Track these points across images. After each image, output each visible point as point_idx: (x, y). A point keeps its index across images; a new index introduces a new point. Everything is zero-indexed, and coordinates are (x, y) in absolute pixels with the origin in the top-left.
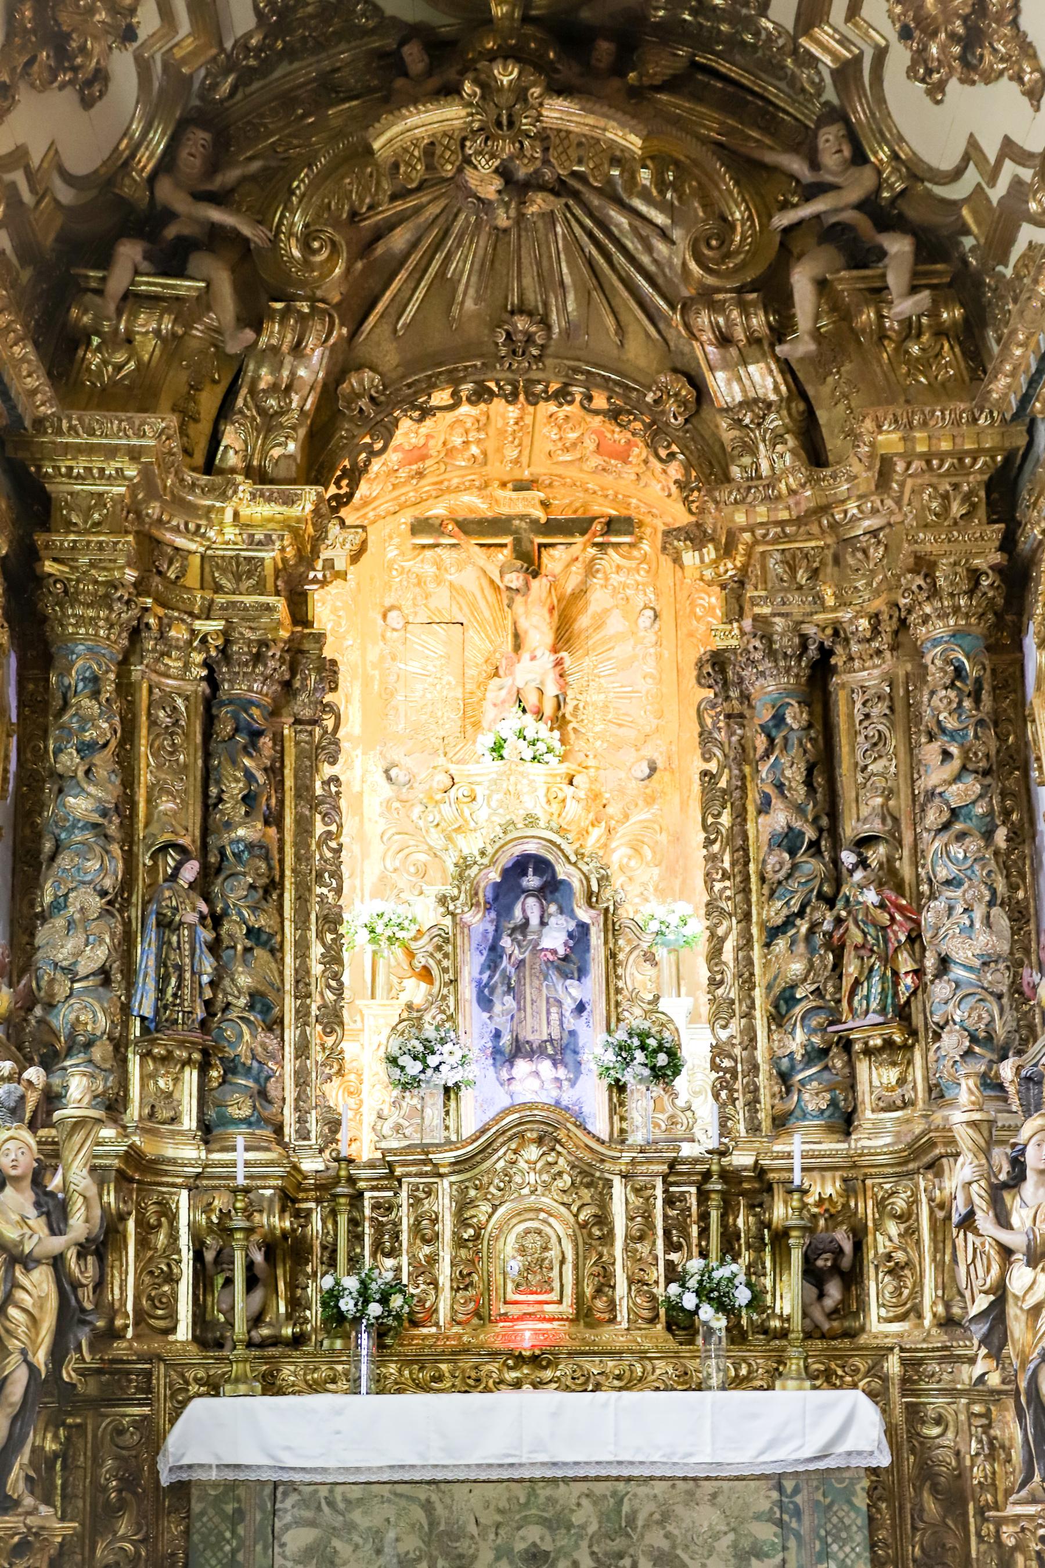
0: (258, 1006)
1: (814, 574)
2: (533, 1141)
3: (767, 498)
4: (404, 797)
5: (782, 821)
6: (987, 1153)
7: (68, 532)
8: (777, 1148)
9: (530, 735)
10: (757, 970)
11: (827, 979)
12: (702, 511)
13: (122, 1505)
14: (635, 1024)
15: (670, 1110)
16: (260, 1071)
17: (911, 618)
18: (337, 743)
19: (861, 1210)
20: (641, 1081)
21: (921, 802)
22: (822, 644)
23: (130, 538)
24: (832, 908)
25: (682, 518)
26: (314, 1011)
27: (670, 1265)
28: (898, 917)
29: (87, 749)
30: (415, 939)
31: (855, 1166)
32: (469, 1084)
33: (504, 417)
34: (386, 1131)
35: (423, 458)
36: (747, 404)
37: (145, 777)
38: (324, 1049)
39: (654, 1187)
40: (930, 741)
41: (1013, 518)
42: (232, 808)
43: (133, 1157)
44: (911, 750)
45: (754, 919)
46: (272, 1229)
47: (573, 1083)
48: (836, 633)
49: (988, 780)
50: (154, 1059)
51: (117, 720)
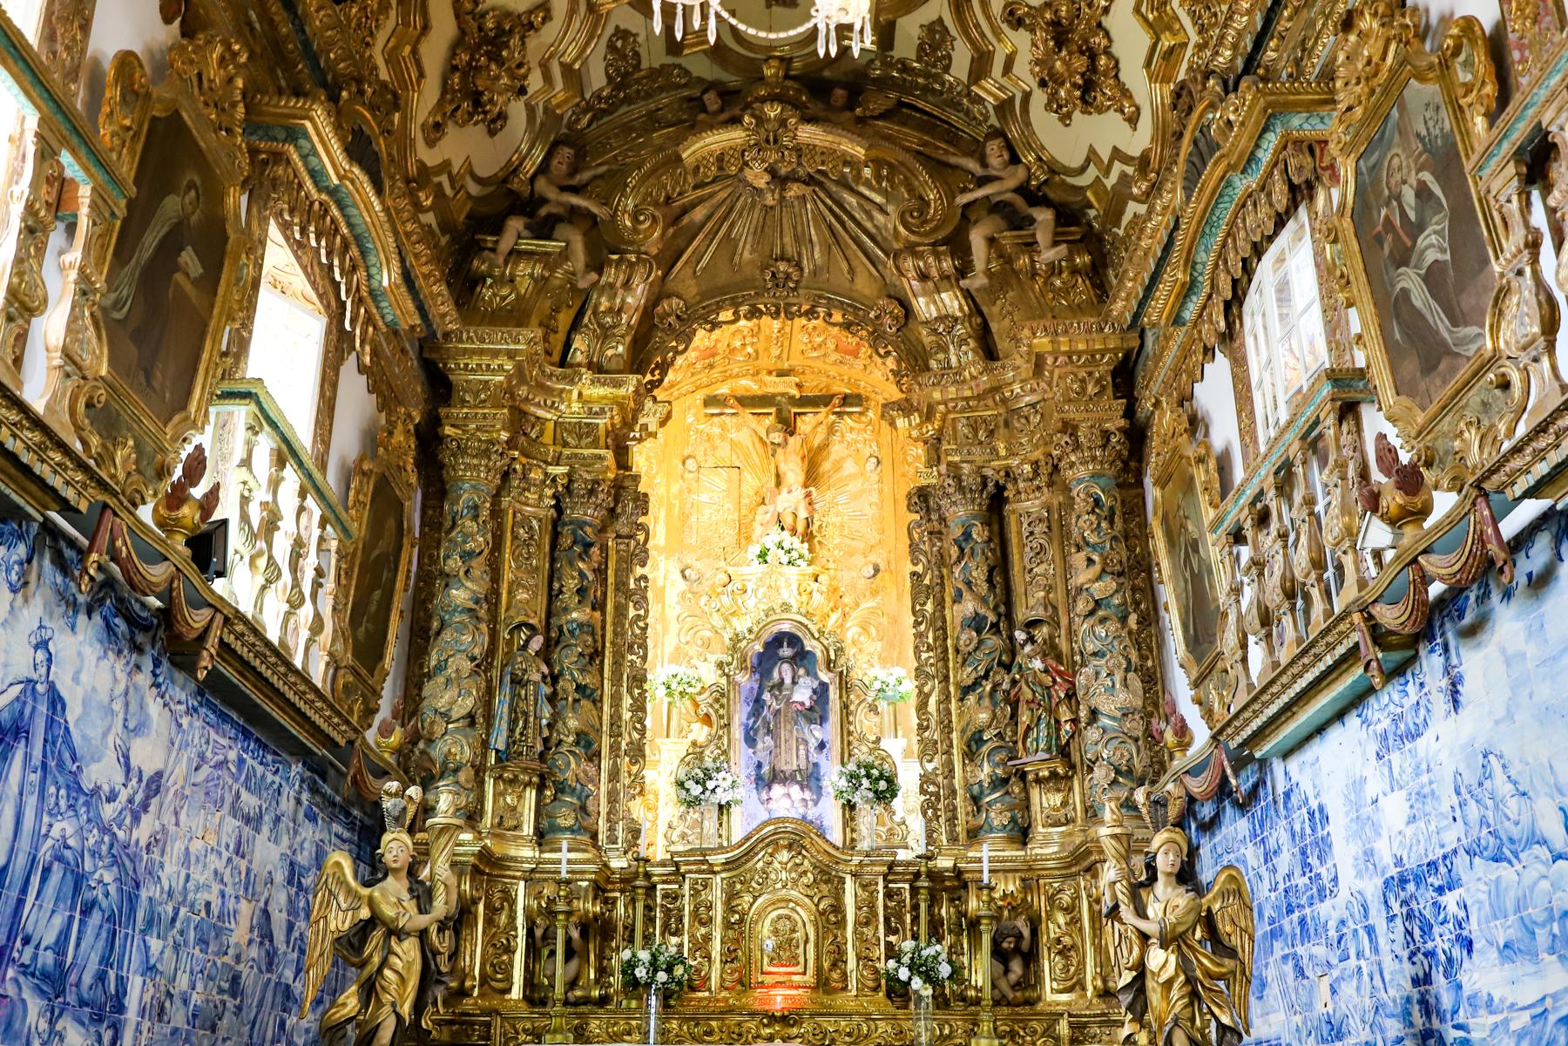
1: (991, 433)
3: (955, 382)
6: (1127, 859)
10: (954, 719)
12: (909, 390)
14: (862, 758)
15: (889, 825)
17: (1062, 464)
18: (646, 551)
20: (867, 801)
21: (1073, 595)
25: (896, 395)
27: (889, 945)
29: (467, 556)
33: (770, 327)
35: (713, 355)
36: (941, 319)
42: (569, 597)
47: (816, 803)
48: (1007, 474)
49: (1122, 580)
51: (489, 536)
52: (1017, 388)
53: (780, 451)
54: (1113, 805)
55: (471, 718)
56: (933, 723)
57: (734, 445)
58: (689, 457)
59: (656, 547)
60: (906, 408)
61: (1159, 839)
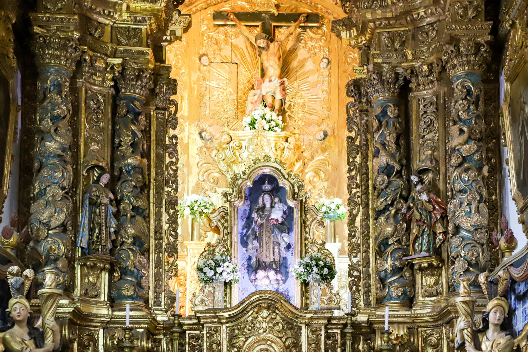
0: (137, 243)
2: (265, 308)
3: (382, 7)
4: (208, 146)
5: (385, 162)
8: (378, 313)
9: (268, 117)
10: (371, 231)
11: (403, 235)
12: (351, 12)
14: (313, 254)
16: (138, 273)
18: (176, 119)
19: (416, 342)
20: (316, 281)
21: (449, 153)
22: (405, 77)
24: (406, 203)
28: (437, 207)
30: (212, 213)
31: (413, 322)
32: (236, 281)
34: (197, 302)
38: (168, 264)
39: (321, 330)
40: (454, 124)
41: (497, 18)
43: (77, 313)
44: (445, 129)
45: (370, 207)
46: (143, 347)
48: (412, 72)
49: (480, 144)
50: (87, 267)
52: (422, 12)
53: (264, 52)
54: (465, 283)
55: (63, 227)
57: (234, 48)
58: (204, 55)
59: (183, 117)
60: (348, 24)
61: (491, 304)
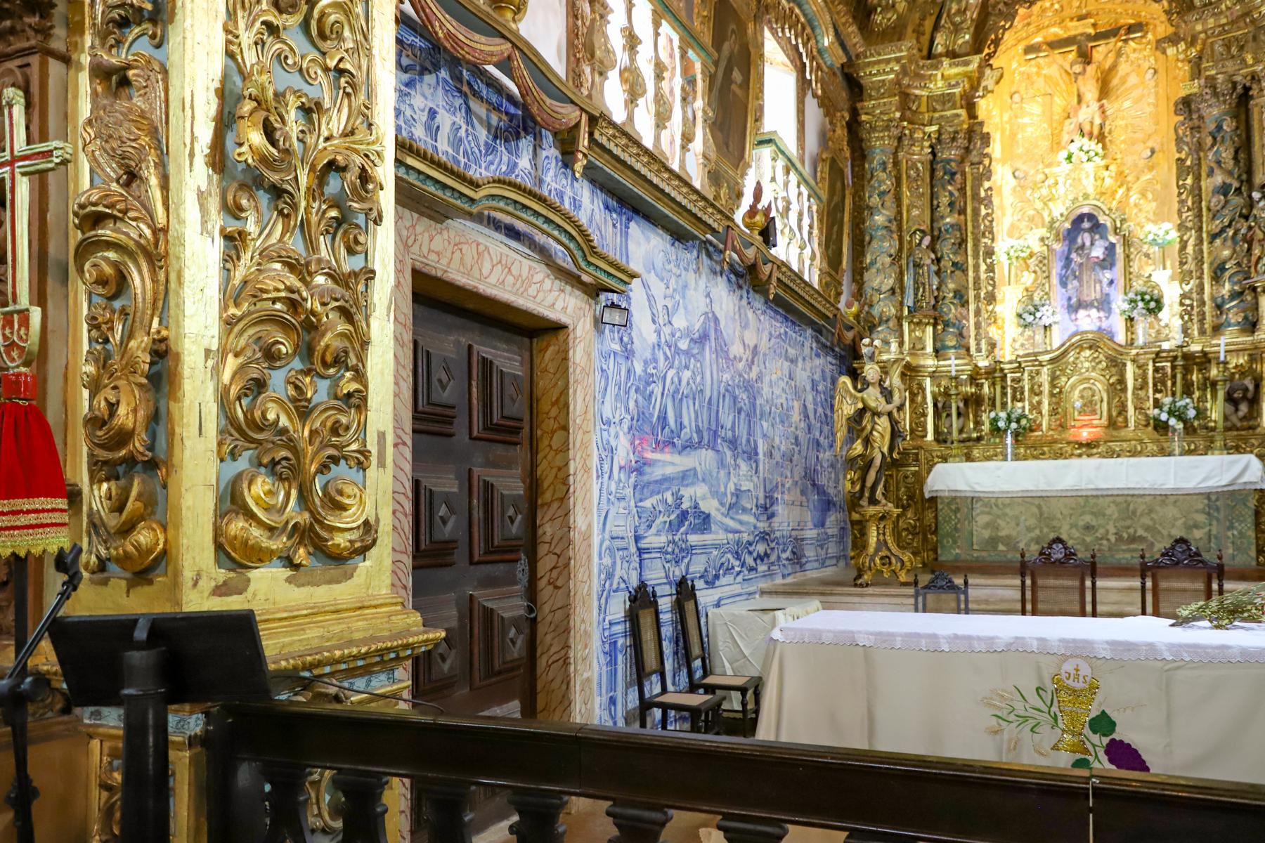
7: (871, 100)
8: (1214, 342)
10: (1205, 255)
13: (909, 506)
15: (1157, 327)
20: (1143, 315)
23: (897, 98)
26: (982, 295)
31: (1256, 348)
37: (906, 202)
42: (944, 209)
46: (967, 392)
56: (1190, 259)
